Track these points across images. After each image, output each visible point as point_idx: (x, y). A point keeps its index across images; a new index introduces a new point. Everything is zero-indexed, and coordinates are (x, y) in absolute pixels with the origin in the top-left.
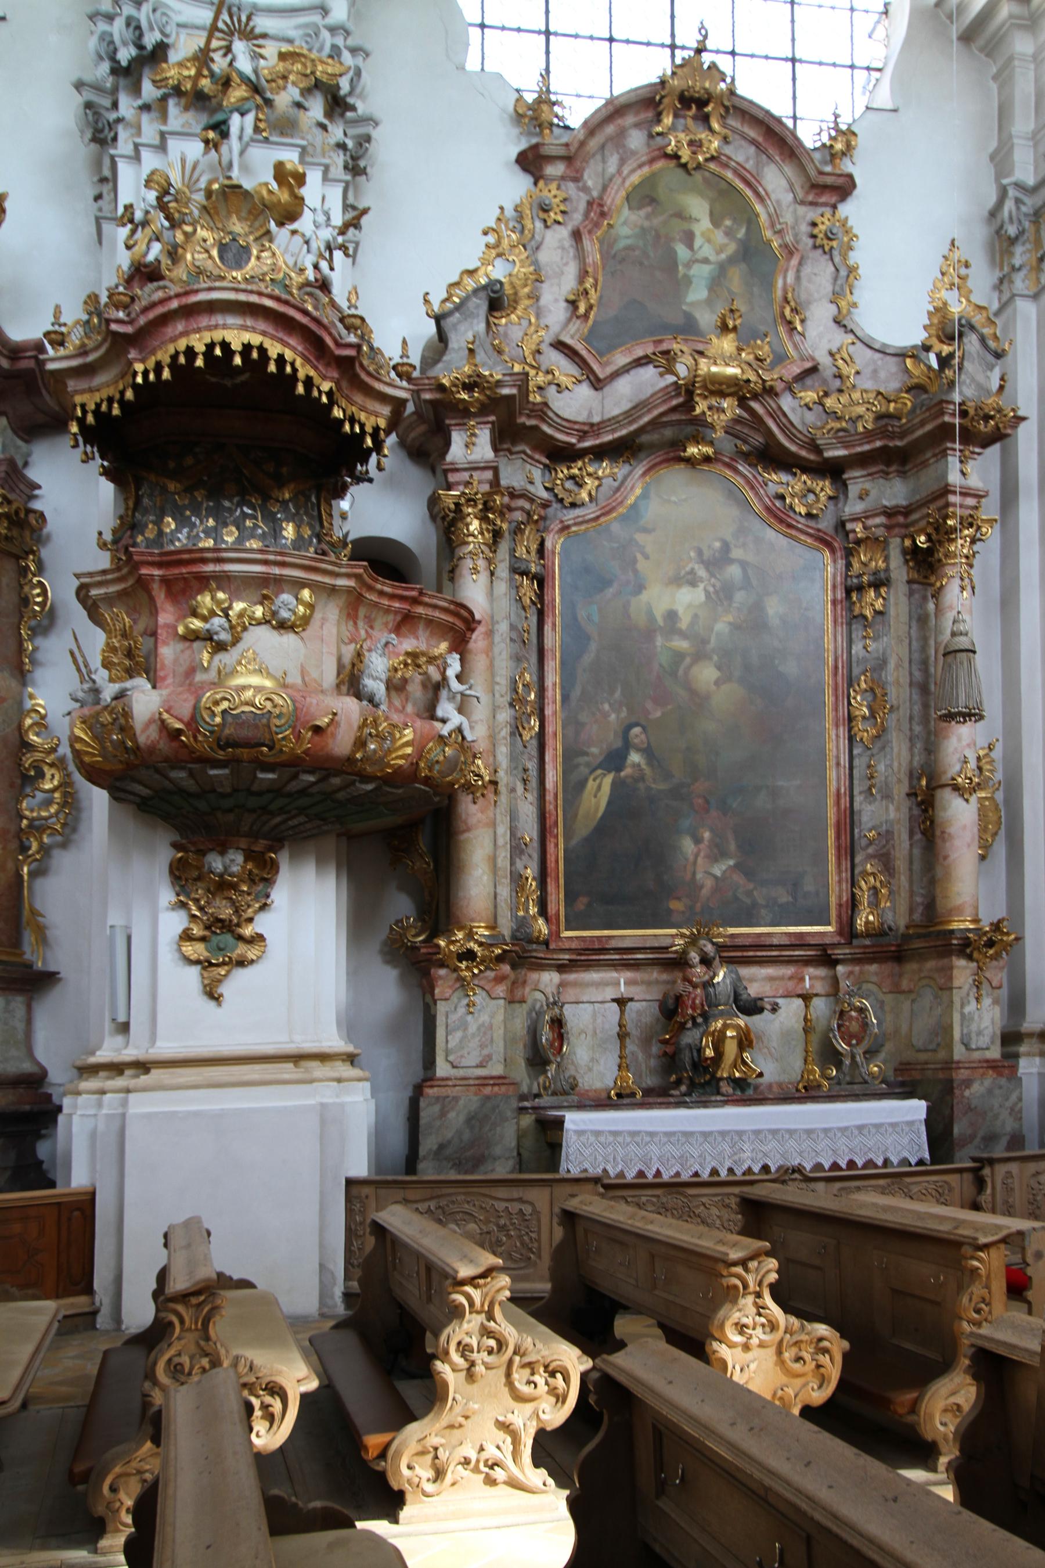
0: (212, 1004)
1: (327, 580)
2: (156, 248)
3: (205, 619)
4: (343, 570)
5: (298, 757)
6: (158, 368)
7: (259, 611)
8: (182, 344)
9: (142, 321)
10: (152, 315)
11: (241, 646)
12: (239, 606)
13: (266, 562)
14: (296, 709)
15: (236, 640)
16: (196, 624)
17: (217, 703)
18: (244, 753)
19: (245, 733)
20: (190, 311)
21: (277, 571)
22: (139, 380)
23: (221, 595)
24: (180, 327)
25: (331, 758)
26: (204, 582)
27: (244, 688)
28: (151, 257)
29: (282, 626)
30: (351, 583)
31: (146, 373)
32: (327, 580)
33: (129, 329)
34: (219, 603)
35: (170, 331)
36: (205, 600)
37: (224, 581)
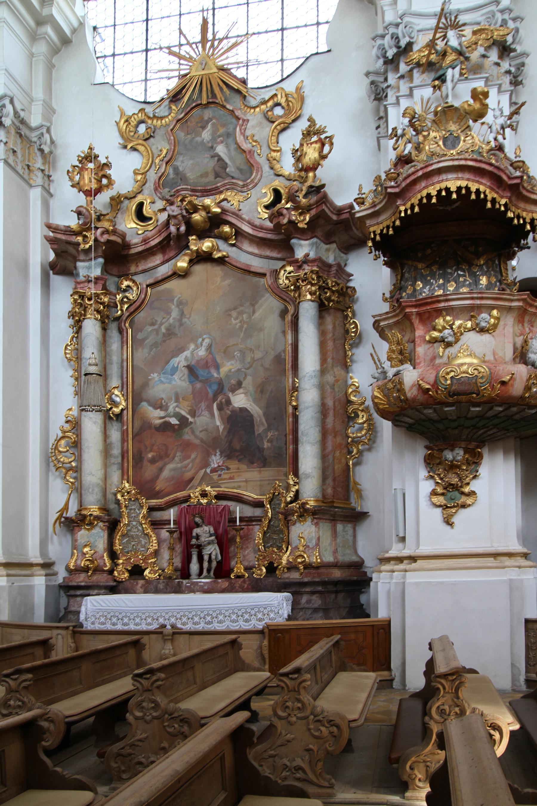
1: (507, 304)
2: (409, 146)
3: (440, 331)
5: (493, 398)
6: (412, 207)
7: (469, 324)
8: (424, 193)
9: (404, 185)
10: (408, 181)
11: (460, 343)
12: (458, 323)
13: (472, 298)
14: (491, 373)
15: (457, 341)
16: (435, 334)
17: (448, 374)
18: (463, 398)
19: (463, 388)
20: (428, 176)
21: (478, 302)
22: (403, 214)
23: (448, 318)
24: (423, 184)
26: (439, 312)
27: (462, 365)
28: (406, 152)
29: (482, 330)
30: (520, 304)
31: (406, 211)
32: (507, 304)
33: (397, 190)
34: (447, 322)
35: (418, 187)
36: (440, 322)
37: (450, 310)
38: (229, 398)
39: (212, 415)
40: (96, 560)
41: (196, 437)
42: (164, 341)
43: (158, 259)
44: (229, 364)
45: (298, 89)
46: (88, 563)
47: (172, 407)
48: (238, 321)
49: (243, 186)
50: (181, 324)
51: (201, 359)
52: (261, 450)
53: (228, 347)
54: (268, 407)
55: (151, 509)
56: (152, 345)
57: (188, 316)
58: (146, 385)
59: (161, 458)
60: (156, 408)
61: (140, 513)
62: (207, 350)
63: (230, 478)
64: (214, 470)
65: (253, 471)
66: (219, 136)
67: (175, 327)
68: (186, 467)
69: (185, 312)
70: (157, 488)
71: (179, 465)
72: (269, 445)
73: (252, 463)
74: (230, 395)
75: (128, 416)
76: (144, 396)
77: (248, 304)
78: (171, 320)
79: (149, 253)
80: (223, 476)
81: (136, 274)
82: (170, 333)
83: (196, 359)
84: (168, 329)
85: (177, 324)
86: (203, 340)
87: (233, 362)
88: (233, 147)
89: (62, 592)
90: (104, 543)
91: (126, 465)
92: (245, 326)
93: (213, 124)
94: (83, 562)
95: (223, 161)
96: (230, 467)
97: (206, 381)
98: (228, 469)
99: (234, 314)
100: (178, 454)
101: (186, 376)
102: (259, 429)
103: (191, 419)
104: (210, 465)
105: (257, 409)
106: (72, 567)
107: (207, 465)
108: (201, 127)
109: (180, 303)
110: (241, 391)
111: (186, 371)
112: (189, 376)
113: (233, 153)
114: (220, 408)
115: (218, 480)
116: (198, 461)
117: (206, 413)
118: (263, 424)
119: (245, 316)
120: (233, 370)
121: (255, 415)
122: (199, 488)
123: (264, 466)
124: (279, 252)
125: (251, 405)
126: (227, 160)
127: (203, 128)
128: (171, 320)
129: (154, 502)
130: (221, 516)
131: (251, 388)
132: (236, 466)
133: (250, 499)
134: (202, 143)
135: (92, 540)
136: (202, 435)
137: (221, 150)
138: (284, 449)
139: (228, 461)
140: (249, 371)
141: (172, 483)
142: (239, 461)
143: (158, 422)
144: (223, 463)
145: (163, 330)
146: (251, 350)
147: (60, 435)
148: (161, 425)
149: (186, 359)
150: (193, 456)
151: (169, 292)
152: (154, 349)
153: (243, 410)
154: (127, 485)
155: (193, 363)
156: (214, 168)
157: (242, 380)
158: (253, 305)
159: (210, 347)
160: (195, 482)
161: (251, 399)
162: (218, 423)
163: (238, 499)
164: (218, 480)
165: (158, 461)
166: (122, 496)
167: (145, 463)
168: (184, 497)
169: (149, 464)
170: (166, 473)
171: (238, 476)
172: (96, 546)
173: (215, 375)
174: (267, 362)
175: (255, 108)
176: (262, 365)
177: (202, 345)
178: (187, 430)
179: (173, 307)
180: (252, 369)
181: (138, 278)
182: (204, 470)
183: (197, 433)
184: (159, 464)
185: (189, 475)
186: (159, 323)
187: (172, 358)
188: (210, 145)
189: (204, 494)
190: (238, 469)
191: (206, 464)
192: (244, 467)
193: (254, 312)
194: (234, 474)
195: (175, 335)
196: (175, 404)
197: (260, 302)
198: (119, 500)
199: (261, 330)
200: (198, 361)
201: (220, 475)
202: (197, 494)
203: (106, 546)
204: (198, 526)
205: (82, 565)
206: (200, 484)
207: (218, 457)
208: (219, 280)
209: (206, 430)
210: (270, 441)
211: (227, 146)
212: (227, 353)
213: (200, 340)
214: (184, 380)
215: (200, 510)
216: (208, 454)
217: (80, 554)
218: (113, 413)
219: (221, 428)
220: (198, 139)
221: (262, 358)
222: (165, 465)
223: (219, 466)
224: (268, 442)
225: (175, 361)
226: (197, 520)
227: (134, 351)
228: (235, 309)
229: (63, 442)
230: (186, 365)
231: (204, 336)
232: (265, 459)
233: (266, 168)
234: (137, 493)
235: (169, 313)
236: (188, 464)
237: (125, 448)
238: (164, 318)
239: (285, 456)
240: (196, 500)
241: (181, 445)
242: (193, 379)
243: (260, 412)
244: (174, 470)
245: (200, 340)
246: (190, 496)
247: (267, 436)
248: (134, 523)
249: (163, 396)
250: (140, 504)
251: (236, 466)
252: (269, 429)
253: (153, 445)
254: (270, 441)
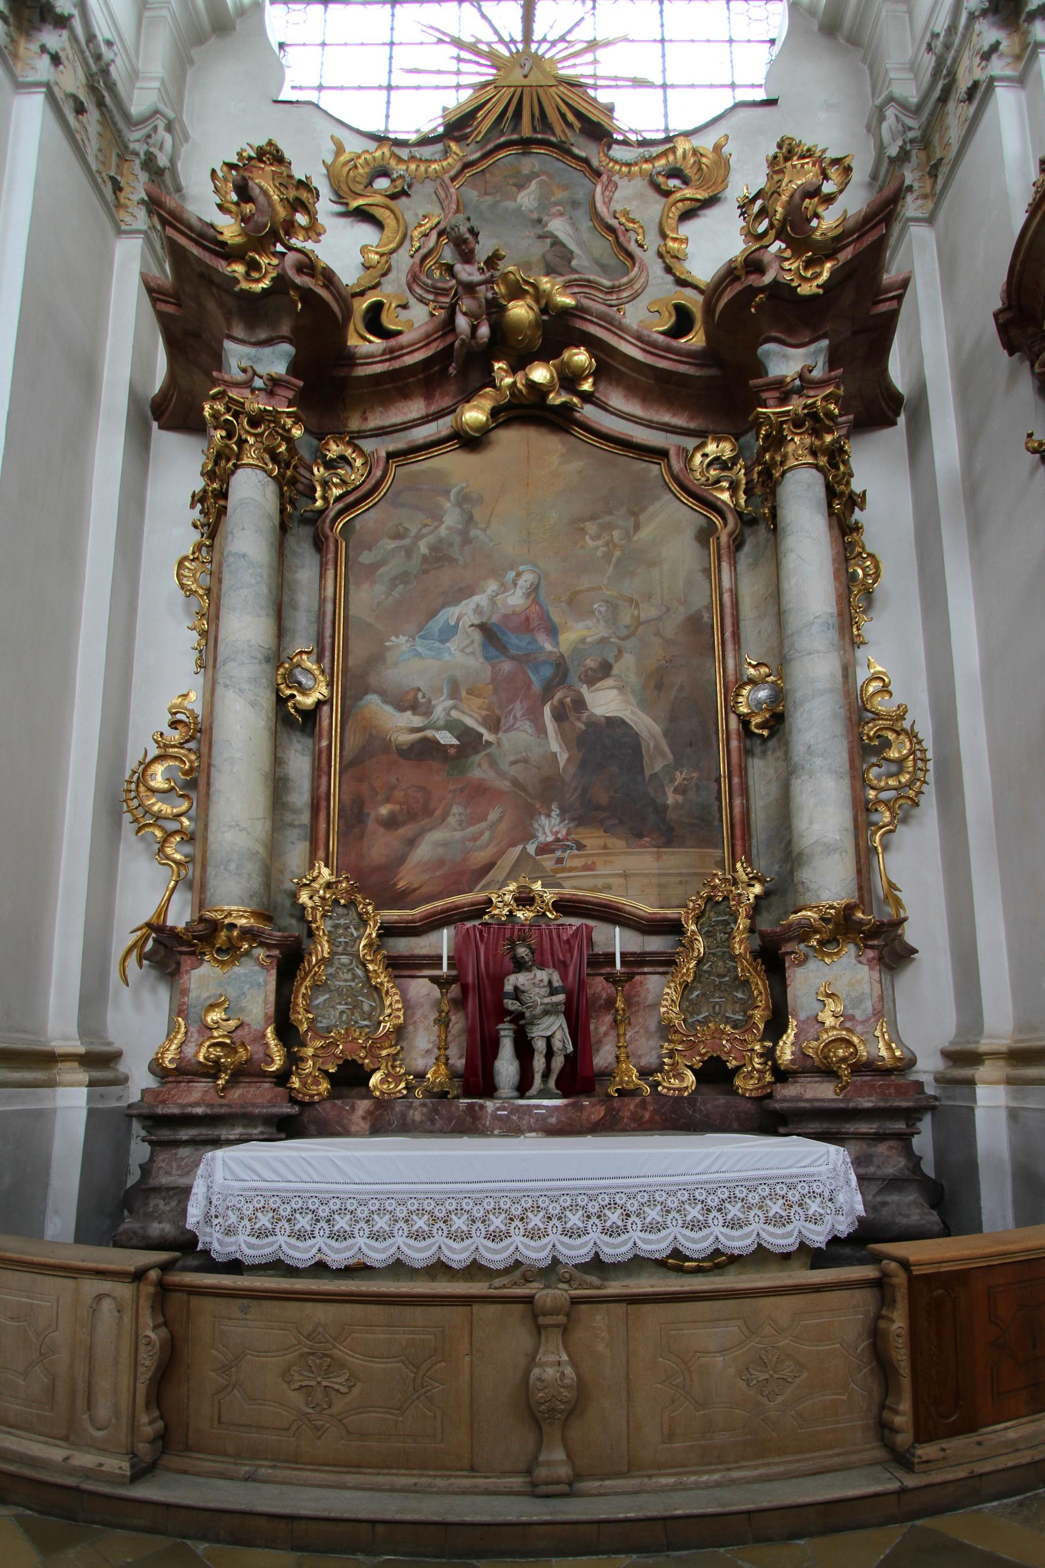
38: (580, 694)
39: (541, 730)
40: (243, 1044)
41: (501, 774)
42: (426, 572)
43: (415, 408)
44: (581, 625)
45: (717, 148)
46: (218, 1052)
47: (441, 708)
48: (600, 543)
49: (611, 290)
50: (466, 541)
51: (514, 613)
52: (661, 810)
53: (577, 593)
54: (673, 718)
55: (388, 931)
56: (395, 578)
57: (483, 525)
58: (377, 658)
59: (412, 816)
60: (401, 708)
61: (360, 938)
62: (528, 595)
63: (586, 868)
65: (640, 853)
66: (556, 204)
67: (451, 545)
68: (475, 839)
69: (477, 517)
70: (401, 885)
71: (458, 835)
72: (680, 798)
73: (640, 836)
74: (584, 689)
75: (331, 720)
76: (373, 680)
77: (623, 510)
78: (443, 531)
80: (568, 863)
81: (362, 435)
82: (439, 556)
83: (503, 611)
84: (433, 548)
85: (457, 540)
86: (519, 575)
87: (589, 623)
88: (585, 224)
89: (137, 1129)
90: (266, 1002)
91: (323, 826)
92: (617, 554)
93: (542, 184)
94: (203, 1050)
95: (564, 246)
96: (584, 842)
97: (527, 659)
98: (580, 847)
99: (592, 528)
100: (456, 809)
101: (477, 647)
102: (656, 765)
103: (487, 736)
104: (537, 837)
105: (648, 721)
106: (167, 1064)
107: (530, 836)
108: (515, 185)
109: (464, 500)
110: (609, 682)
111: (477, 636)
112: (484, 646)
113: (586, 235)
114: (559, 716)
115: (556, 871)
116: (503, 826)
117: (527, 726)
118: (662, 754)
119: (616, 533)
120: (589, 640)
121: (644, 735)
122: (512, 887)
123: (668, 844)
124: (692, 418)
125: (633, 713)
126: (572, 245)
127: (521, 187)
128: (443, 531)
129: (393, 915)
130: (571, 951)
131: (633, 679)
132: (601, 842)
133: (642, 913)
134: (518, 212)
135: (232, 993)
136: (513, 771)
137: (558, 226)
138: (715, 808)
139: (580, 830)
140: (628, 644)
141: (439, 873)
142: (605, 832)
143: (406, 738)
144: (568, 833)
145: (423, 548)
146: (631, 601)
147: (154, 751)
148: (413, 746)
149: (478, 610)
150: (493, 816)
151: (439, 475)
152: (401, 587)
153: (614, 723)
154: (326, 872)
155: (495, 619)
156: (544, 257)
157: (611, 660)
158: (635, 515)
159: (534, 590)
160: (498, 873)
161: (632, 700)
162: (555, 745)
163: (611, 915)
164: (556, 871)
165: (404, 823)
166: (311, 898)
167: (371, 824)
168: (473, 904)
169: (382, 830)
170: (424, 851)
171: (606, 863)
172: (242, 1009)
173: (548, 647)
174: (671, 627)
175: (628, 165)
176: (658, 634)
177: (515, 585)
179: (448, 505)
180: (633, 639)
181: (367, 445)
182: (521, 847)
183: (504, 766)
184: (406, 831)
185: (481, 857)
186: (413, 533)
187: (443, 607)
188: (535, 216)
189: (525, 899)
190: (605, 847)
192: (619, 844)
193: (637, 527)
194: (595, 859)
195: (452, 560)
196: (450, 703)
197: (651, 509)
198: (303, 907)
199: (653, 564)
200: (506, 617)
201: (560, 860)
202: (508, 898)
203: (271, 1009)
204: (520, 966)
205: (201, 1059)
206: (511, 876)
207: (555, 818)
208: (555, 460)
209: (526, 761)
210: (681, 790)
211: (573, 223)
212: (575, 603)
213: (512, 574)
214: (472, 653)
215: (519, 934)
216: (532, 813)
217: (193, 1029)
218: (295, 707)
219: (563, 758)
220: (510, 205)
221: (659, 619)
222: (422, 832)
223: (557, 840)
224: (676, 791)
225: (450, 614)
226: (522, 951)
227: (352, 587)
228: (593, 518)
229: (159, 769)
230: (476, 622)
231: (521, 568)
232: (671, 829)
233: (656, 268)
234: (350, 891)
235: (439, 518)
236: (481, 834)
237: (323, 789)
238: (426, 525)
239: (716, 823)
240: (505, 911)
241: (462, 790)
242: (493, 652)
243: (657, 729)
244: (445, 844)
245: (512, 574)
246: (489, 902)
247: (672, 780)
248: (345, 959)
249: (421, 684)
250: (360, 915)
251: (601, 842)
252: (678, 764)
253: (394, 788)
254: (681, 790)
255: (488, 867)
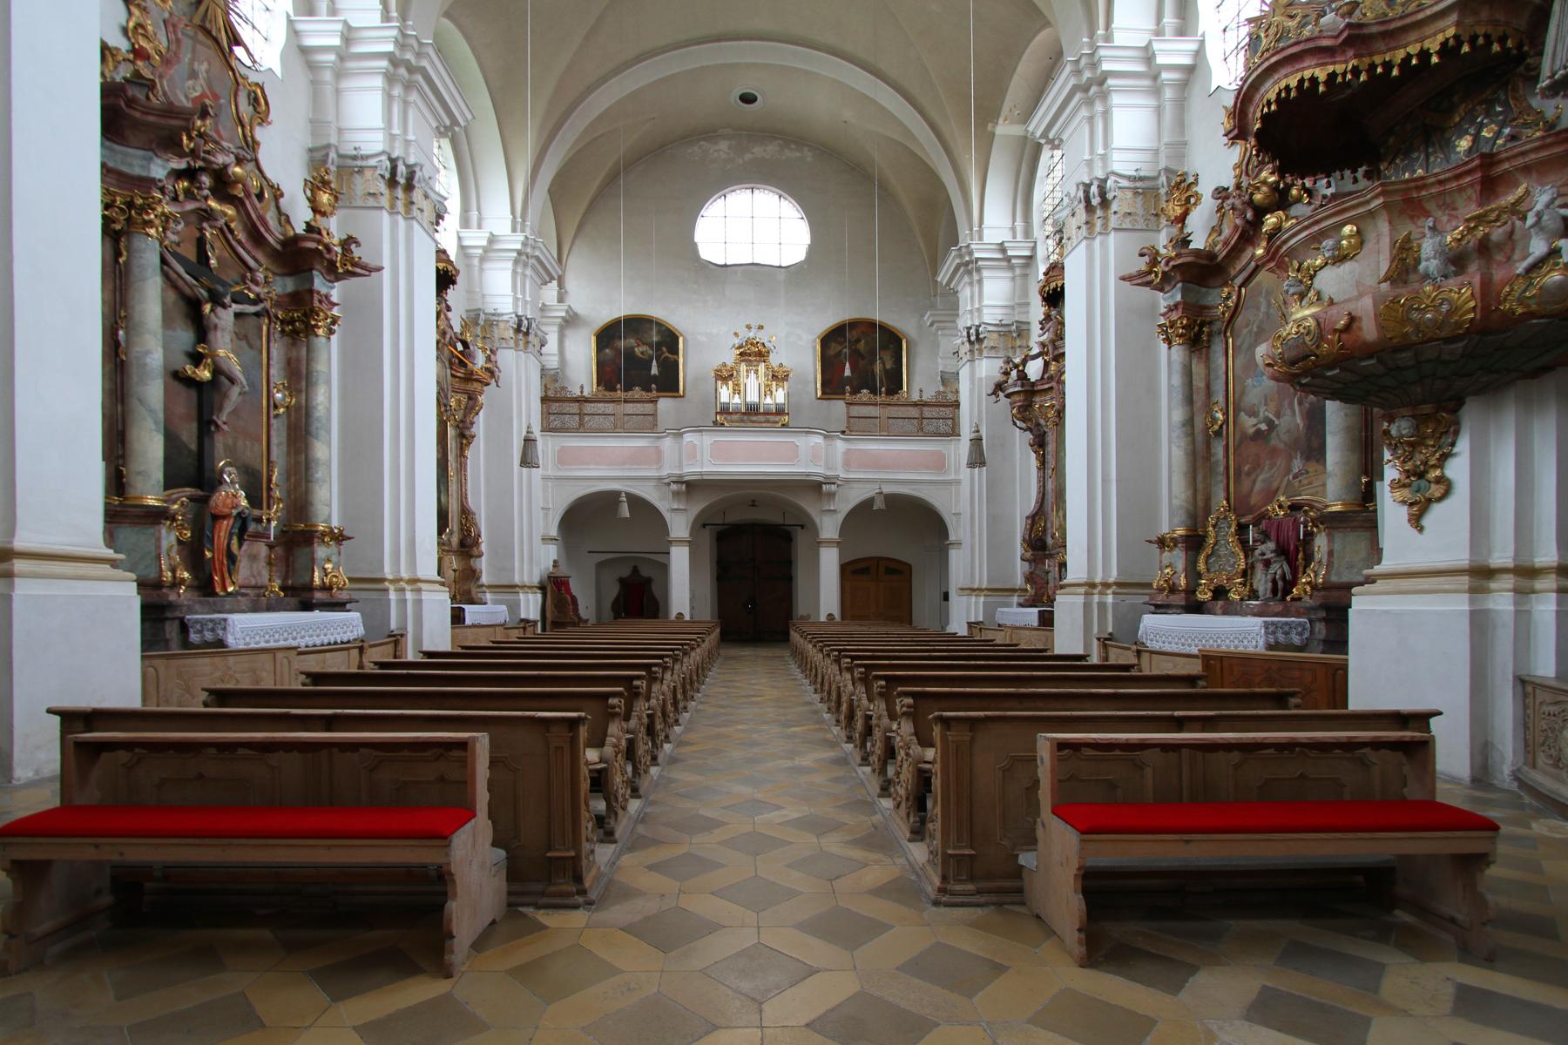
0: (1415, 531)
1: (1361, 210)
4: (1369, 196)
13: (1306, 228)
14: (1319, 324)
21: (1316, 228)
25: (1366, 344)
30: (1380, 200)
32: (1361, 210)
63: (1310, 483)
64: (1295, 477)
68: (1272, 476)
71: (1268, 475)
79: (1235, 251)
84: (1258, 327)
100: (1268, 462)
145: (1255, 329)
162: (1299, 420)
170: (1258, 486)
178: (1274, 434)
184: (1253, 477)
185: (1275, 485)
191: (1288, 470)
201: (1300, 481)
216: (1290, 458)
219: (1301, 426)
222: (1257, 476)
235: (1258, 309)
244: (1264, 481)
255: (1278, 489)
